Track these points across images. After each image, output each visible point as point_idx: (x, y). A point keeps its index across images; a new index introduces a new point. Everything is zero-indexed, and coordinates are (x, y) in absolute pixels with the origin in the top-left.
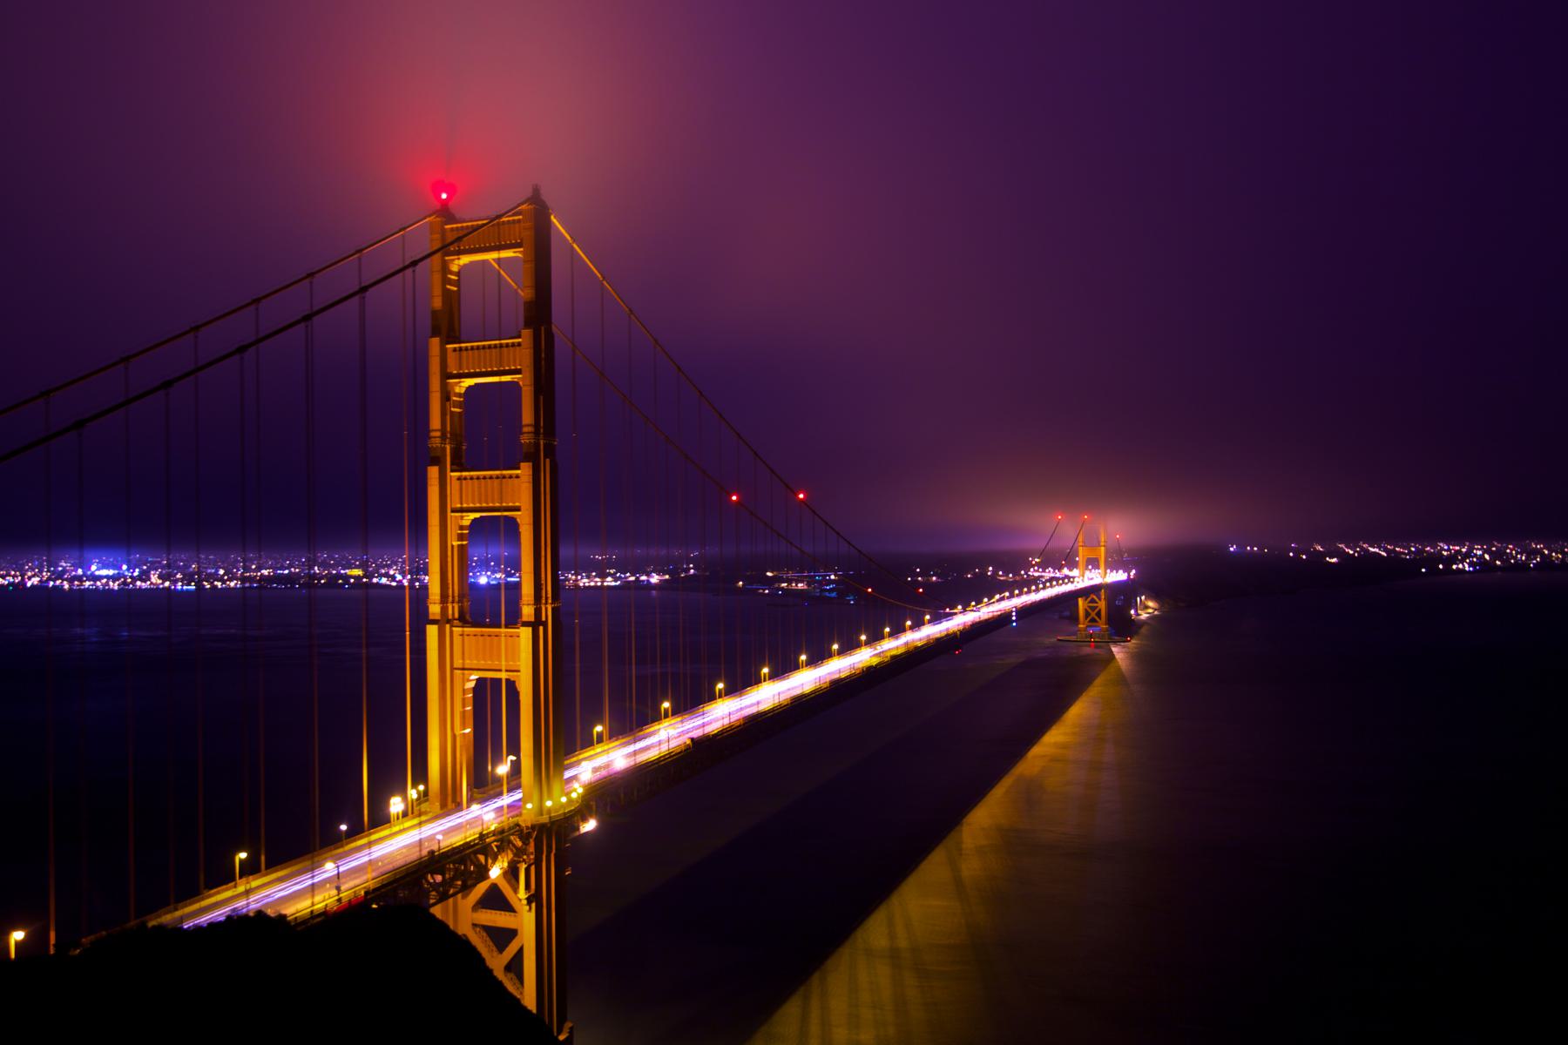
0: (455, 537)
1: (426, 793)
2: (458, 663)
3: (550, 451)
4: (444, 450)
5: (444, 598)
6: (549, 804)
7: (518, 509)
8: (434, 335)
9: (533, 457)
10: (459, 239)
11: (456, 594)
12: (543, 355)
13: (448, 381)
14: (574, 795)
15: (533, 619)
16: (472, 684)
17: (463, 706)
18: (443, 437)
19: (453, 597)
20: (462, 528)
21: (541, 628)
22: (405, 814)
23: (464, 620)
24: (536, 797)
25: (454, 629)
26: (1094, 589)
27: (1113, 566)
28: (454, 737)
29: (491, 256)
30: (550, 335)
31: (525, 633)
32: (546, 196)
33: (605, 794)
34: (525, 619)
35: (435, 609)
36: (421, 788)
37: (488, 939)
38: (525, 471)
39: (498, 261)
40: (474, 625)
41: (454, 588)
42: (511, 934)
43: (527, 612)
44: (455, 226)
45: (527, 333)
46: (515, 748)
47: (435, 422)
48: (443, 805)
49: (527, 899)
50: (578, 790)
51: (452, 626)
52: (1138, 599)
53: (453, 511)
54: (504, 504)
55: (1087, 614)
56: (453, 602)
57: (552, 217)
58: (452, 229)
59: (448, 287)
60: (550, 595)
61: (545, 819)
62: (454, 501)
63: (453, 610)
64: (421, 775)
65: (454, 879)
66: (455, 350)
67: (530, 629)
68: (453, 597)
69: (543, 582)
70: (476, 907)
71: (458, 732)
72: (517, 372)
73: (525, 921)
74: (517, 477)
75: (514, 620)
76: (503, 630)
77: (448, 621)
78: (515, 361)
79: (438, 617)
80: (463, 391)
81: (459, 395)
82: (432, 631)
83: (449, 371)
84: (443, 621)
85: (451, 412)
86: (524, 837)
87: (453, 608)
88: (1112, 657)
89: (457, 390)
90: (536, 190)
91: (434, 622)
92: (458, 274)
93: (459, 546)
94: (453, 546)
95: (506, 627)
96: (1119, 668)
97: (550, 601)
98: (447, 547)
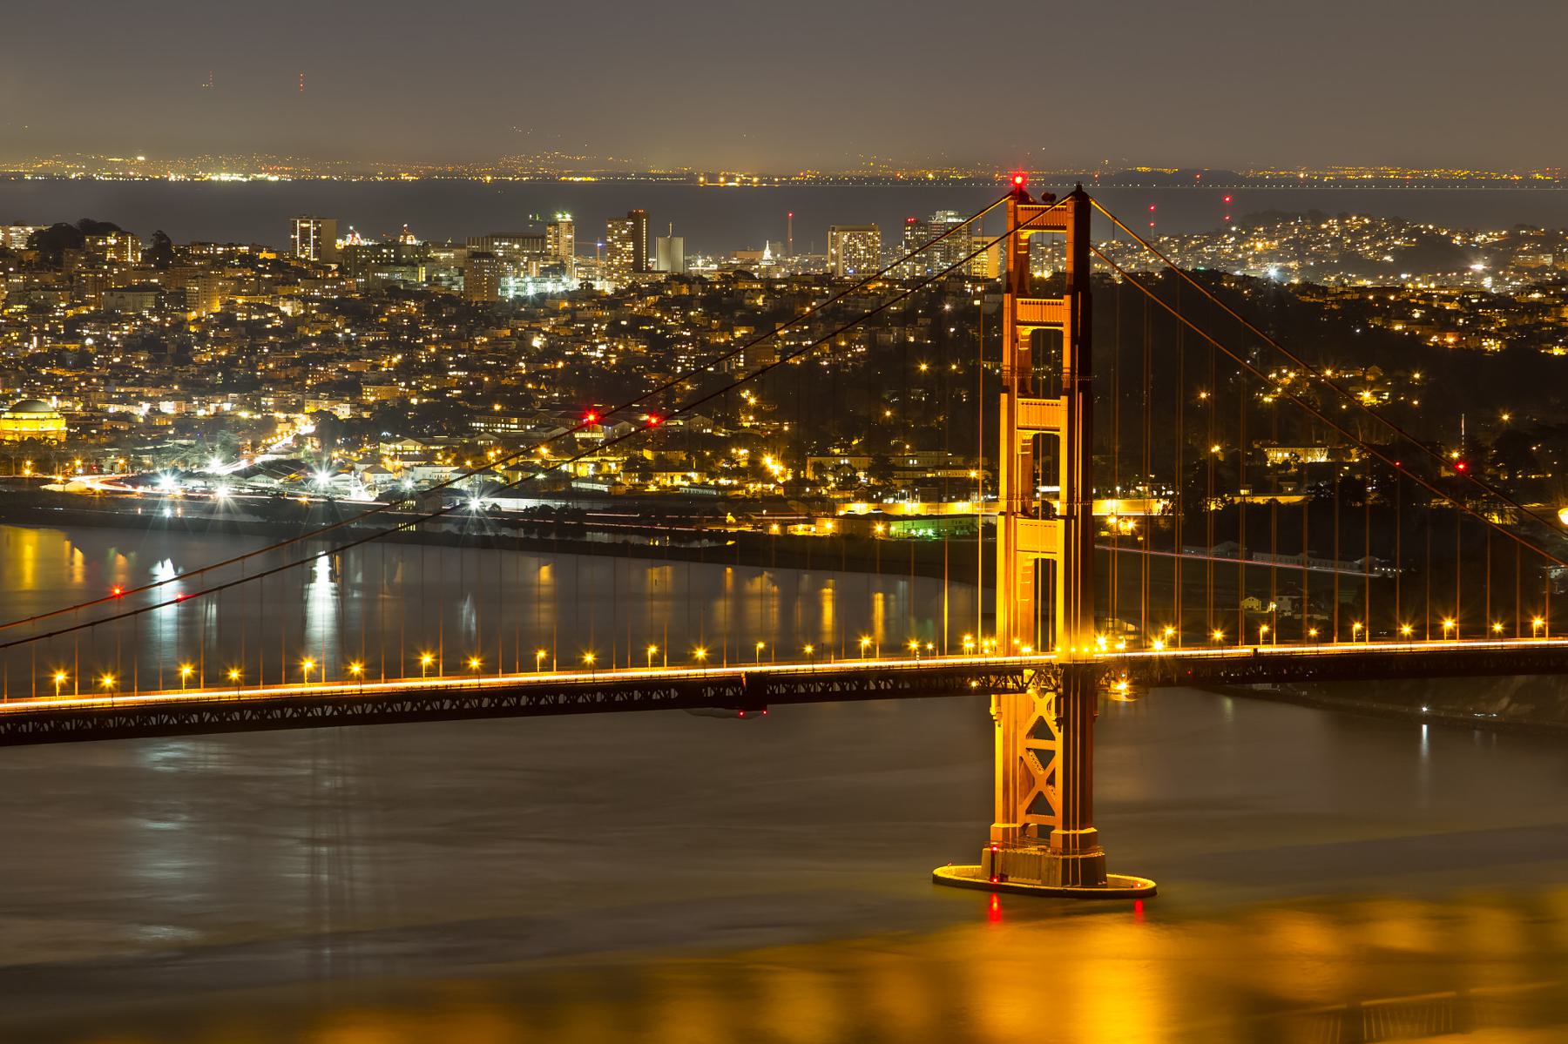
0: (1019, 449)
3: (1084, 387)
4: (1012, 381)
6: (1073, 650)
7: (1058, 430)
8: (1009, 290)
11: (1020, 493)
12: (1079, 314)
13: (1017, 326)
15: (1066, 514)
16: (1032, 564)
19: (1017, 495)
20: (1024, 441)
21: (1073, 521)
23: (1025, 512)
28: (1016, 603)
31: (1061, 523)
32: (1087, 188)
37: (1038, 762)
38: (1064, 400)
42: (1052, 753)
44: (1024, 206)
49: (1056, 720)
51: (1016, 517)
53: (1018, 428)
54: (1043, 425)
56: (1017, 499)
57: (1093, 203)
58: (1022, 209)
59: (1019, 252)
60: (1080, 496)
62: (1021, 420)
66: (1022, 303)
68: (1017, 495)
69: (1075, 487)
70: (1029, 736)
71: (1019, 600)
72: (1061, 325)
73: (1057, 745)
76: (1040, 521)
77: (1013, 514)
78: (1061, 317)
79: (1005, 511)
80: (1029, 333)
81: (1023, 337)
83: (1018, 318)
85: (1019, 350)
87: (1017, 503)
90: (1079, 187)
91: (1001, 514)
92: (1028, 241)
93: (1022, 455)
95: (1043, 519)
97: (1080, 500)
98: (1013, 456)
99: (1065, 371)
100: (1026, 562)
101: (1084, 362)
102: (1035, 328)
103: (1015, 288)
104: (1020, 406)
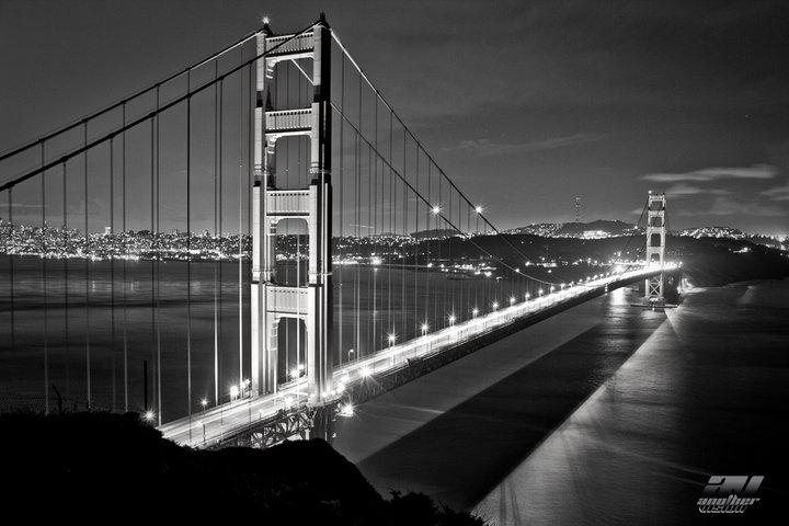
1: (250, 386)
2: (270, 308)
4: (263, 177)
5: (262, 268)
6: (324, 395)
8: (259, 104)
9: (316, 182)
10: (277, 47)
16: (278, 321)
17: (271, 334)
18: (263, 169)
22: (239, 398)
23: (272, 281)
24: (316, 392)
25: (269, 288)
26: (657, 274)
27: (667, 257)
28: (267, 352)
29: (292, 57)
30: (329, 108)
33: (358, 393)
34: (311, 282)
35: (256, 275)
36: (248, 382)
39: (299, 60)
40: (279, 286)
41: (268, 262)
43: (313, 278)
45: (316, 106)
46: (303, 359)
47: (258, 160)
48: (261, 393)
50: (341, 389)
55: (651, 289)
61: (321, 404)
62: (269, 209)
63: (267, 276)
64: (248, 373)
65: (268, 436)
67: (313, 289)
75: (304, 282)
80: (274, 140)
82: (254, 288)
84: (261, 282)
86: (310, 414)
88: (666, 317)
96: (669, 324)
99: (313, 165)
100: (273, 321)
101: (326, 162)
102: (280, 135)
103: (264, 103)
104: (269, 197)
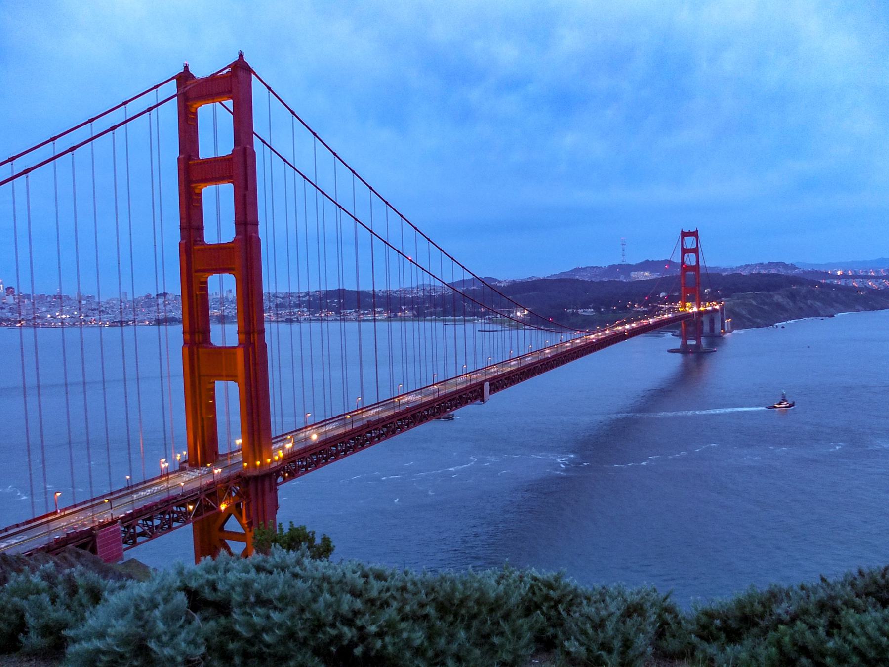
14: (276, 458)
28: (202, 420)
51: (198, 348)
52: (726, 321)
53: (196, 271)
74: (233, 248)
89: (197, 191)
90: (241, 56)
93: (201, 294)
94: (196, 295)
